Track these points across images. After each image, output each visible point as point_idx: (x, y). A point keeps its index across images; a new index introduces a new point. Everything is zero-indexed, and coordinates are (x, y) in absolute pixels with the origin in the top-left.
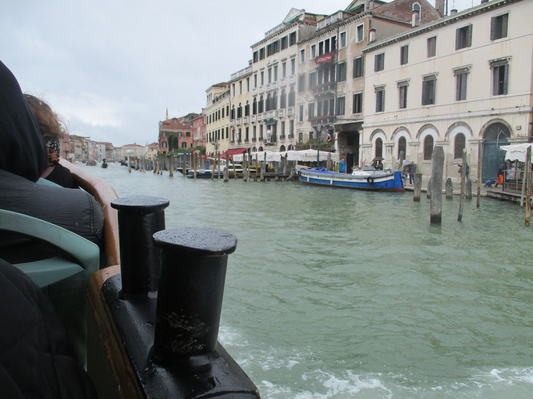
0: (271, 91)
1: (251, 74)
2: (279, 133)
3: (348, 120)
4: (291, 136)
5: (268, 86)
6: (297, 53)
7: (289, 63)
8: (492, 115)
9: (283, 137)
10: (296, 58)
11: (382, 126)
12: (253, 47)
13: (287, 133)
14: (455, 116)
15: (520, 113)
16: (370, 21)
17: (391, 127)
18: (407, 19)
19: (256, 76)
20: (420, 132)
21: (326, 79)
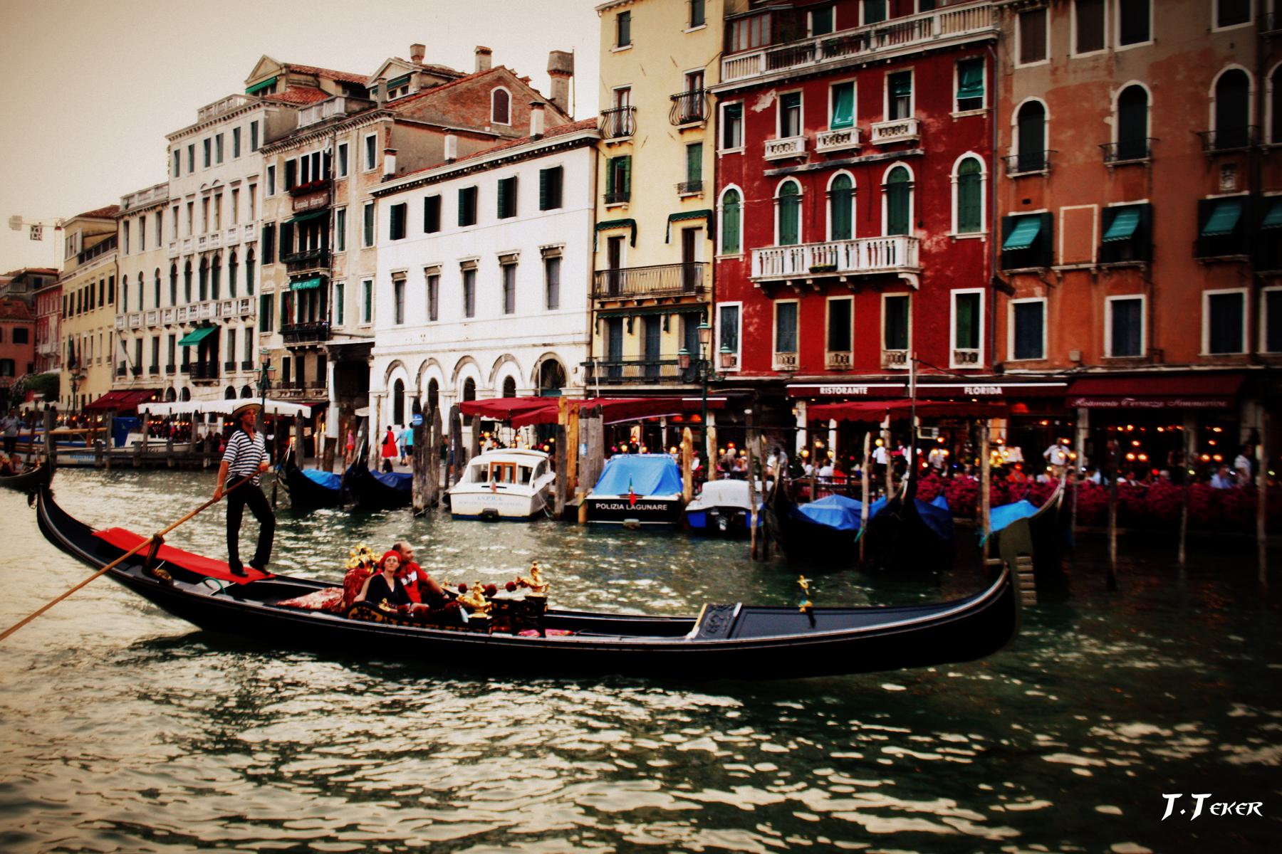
0: (208, 251)
1: (166, 204)
2: (223, 357)
3: (351, 336)
4: (248, 365)
5: (202, 239)
6: (261, 173)
7: (244, 188)
8: (545, 345)
9: (231, 366)
10: (259, 181)
11: (403, 353)
12: (173, 137)
13: (240, 357)
14: (500, 344)
15: (574, 344)
16: (388, 130)
17: (416, 356)
18: (479, 122)
19: (176, 209)
20: (457, 369)
21: (314, 244)
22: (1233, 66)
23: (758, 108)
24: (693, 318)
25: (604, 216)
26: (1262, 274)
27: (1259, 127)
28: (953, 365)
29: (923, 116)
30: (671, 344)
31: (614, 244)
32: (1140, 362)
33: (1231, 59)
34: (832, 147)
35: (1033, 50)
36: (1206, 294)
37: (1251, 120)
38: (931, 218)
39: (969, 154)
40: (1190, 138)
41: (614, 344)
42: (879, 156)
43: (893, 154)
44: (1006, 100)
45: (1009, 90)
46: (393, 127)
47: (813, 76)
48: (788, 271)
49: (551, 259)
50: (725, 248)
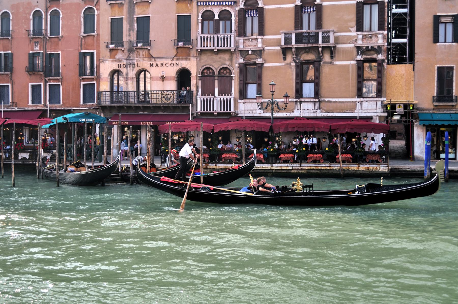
22: (38, 9)
26: (47, 78)
27: (46, 30)
33: (37, 6)
36: (30, 84)
37: (43, 28)
40: (24, 32)
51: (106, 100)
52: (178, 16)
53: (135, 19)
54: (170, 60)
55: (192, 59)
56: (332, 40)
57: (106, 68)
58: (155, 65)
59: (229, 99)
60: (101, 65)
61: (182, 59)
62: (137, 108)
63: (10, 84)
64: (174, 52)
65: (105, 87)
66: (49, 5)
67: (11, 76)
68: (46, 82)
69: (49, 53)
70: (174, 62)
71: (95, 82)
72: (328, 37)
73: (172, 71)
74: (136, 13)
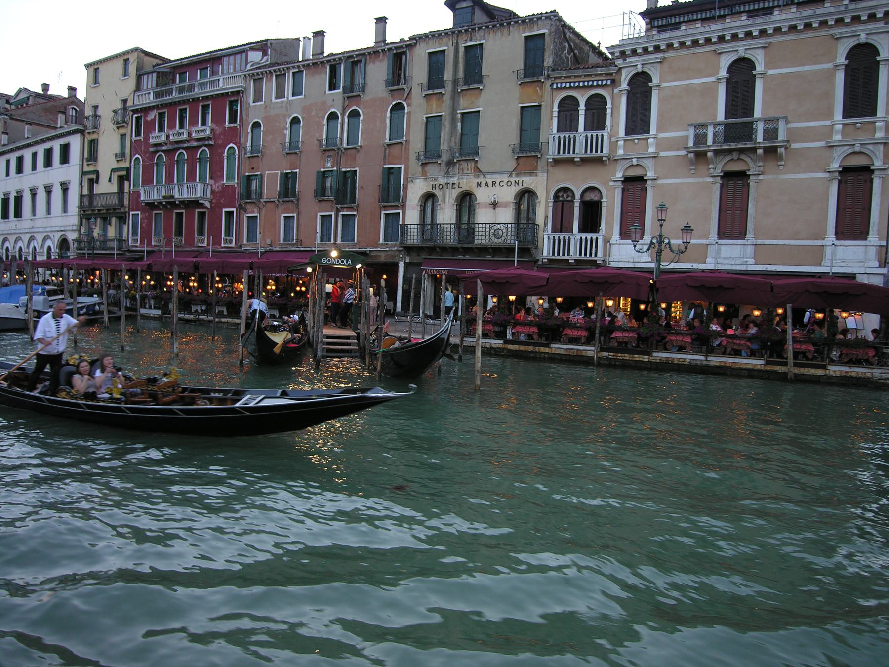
16: (5, 122)
22: (333, 110)
23: (149, 118)
24: (122, 219)
25: (86, 169)
26: (339, 206)
27: (341, 139)
28: (223, 245)
29: (214, 126)
30: (111, 232)
31: (92, 183)
32: (293, 245)
33: (332, 106)
34: (176, 139)
35: (258, 98)
38: (216, 174)
39: (231, 145)
40: (316, 142)
41: (90, 231)
42: (195, 144)
43: (200, 143)
44: (247, 120)
45: (248, 115)
46: (9, 121)
47: (171, 103)
48: (155, 197)
49: (65, 188)
50: (134, 186)
51: (413, 237)
52: (522, 107)
53: (459, 116)
54: (506, 176)
55: (540, 175)
56: (782, 136)
57: (416, 190)
58: (483, 184)
59: (594, 238)
60: (410, 186)
61: (525, 174)
62: (454, 250)
63: (295, 215)
64: (512, 164)
65: (412, 217)
66: (347, 103)
67: (298, 204)
68: (338, 211)
69: (343, 170)
70: (513, 180)
71: (400, 211)
72: (776, 131)
73: (508, 194)
74: (461, 107)
